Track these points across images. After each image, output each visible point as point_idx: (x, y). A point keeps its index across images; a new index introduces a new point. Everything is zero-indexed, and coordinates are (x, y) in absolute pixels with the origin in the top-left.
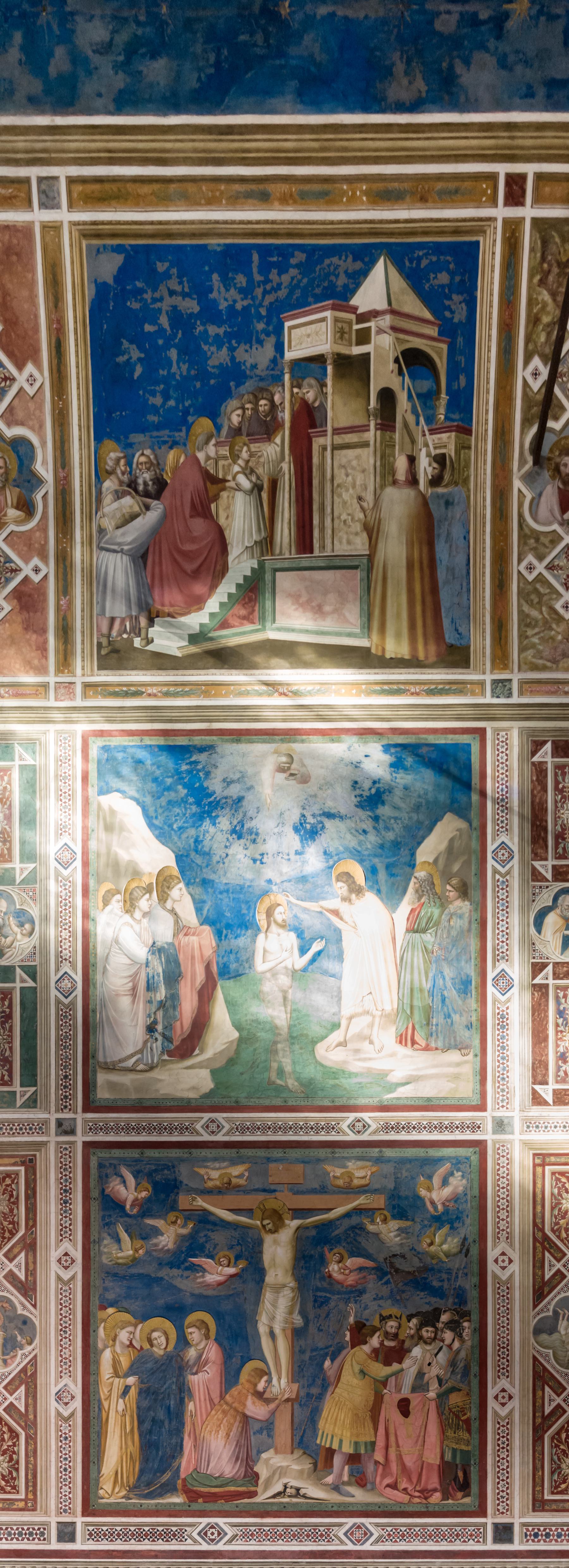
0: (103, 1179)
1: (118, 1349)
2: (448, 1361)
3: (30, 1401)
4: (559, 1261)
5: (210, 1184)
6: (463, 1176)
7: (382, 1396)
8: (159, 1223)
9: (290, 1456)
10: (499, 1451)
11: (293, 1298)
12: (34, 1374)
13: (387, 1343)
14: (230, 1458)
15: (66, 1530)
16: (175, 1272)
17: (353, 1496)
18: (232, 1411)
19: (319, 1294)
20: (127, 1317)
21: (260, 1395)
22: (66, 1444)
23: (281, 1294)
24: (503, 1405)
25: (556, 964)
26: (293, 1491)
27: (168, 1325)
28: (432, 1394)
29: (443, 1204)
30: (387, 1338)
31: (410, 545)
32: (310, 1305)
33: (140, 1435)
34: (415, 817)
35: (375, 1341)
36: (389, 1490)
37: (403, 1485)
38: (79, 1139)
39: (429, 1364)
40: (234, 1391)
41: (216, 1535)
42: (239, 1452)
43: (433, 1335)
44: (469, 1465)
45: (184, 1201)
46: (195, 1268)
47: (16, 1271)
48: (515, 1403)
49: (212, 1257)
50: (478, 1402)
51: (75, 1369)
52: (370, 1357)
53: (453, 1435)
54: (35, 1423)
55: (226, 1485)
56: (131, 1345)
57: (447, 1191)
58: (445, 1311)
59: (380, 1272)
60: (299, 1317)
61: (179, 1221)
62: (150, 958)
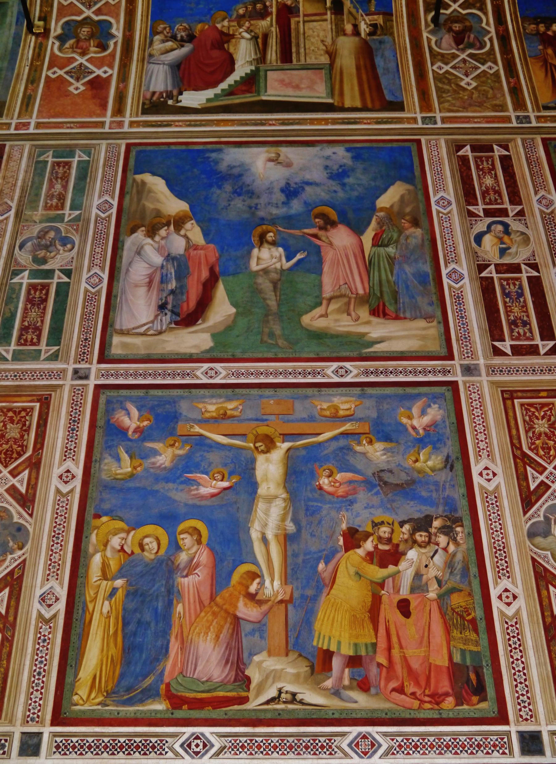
0: (109, 412)
1: (109, 553)
2: (446, 563)
3: (13, 603)
4: (541, 473)
5: (207, 415)
6: (440, 408)
7: (380, 597)
8: (158, 446)
9: (284, 659)
10: (511, 651)
11: (285, 508)
12: (21, 578)
13: (381, 547)
14: (220, 661)
15: (30, 742)
16: (171, 485)
17: (356, 702)
18: (222, 613)
19: (311, 503)
20: (121, 524)
21: (252, 597)
22: (43, 646)
23: (273, 504)
24: (509, 604)
25: (496, 265)
26: (289, 697)
27: (160, 532)
28: (432, 595)
29: (424, 429)
30: (381, 543)
31: (357, 59)
32: (302, 514)
33: (124, 637)
34: (373, 184)
35: (369, 545)
36: (395, 695)
37: (410, 688)
38: (92, 382)
39: (426, 566)
40: (225, 593)
41: (201, 747)
42: (229, 655)
43: (427, 539)
44: (481, 667)
45: (182, 428)
46: (189, 482)
47: (18, 485)
48: (520, 603)
49: (207, 473)
50: (481, 601)
51: (63, 572)
52: (364, 559)
53: (459, 635)
54: (14, 625)
55: (215, 690)
56: (122, 549)
57: (426, 420)
58: (436, 518)
59: (369, 485)
60: (291, 524)
61: (177, 444)
62: (165, 263)
